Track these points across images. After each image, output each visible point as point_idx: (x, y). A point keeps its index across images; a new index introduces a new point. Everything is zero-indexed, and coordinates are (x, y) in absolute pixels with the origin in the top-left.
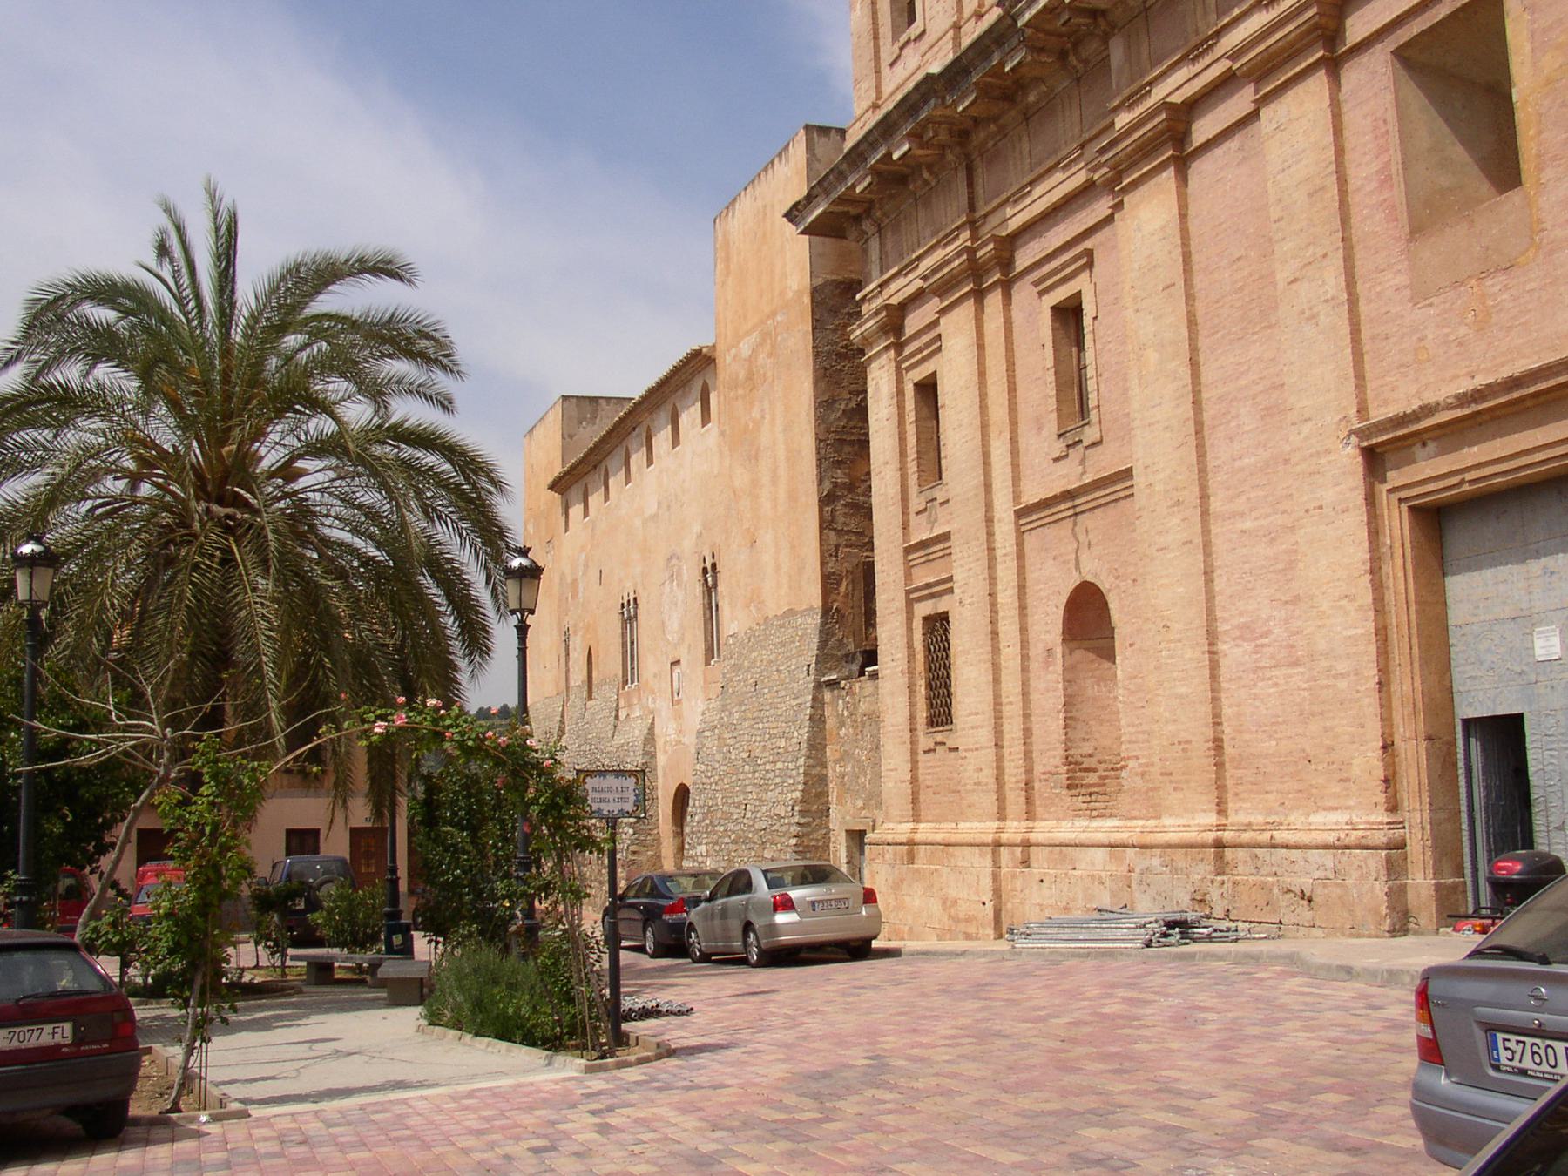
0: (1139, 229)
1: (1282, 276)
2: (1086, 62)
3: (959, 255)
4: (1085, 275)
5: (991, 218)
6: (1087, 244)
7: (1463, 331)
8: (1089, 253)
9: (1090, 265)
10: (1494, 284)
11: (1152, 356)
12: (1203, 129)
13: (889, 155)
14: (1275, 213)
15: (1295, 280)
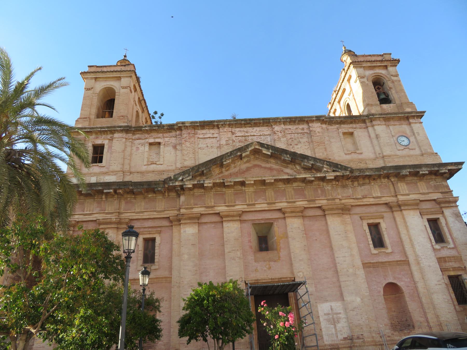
0: (185, 232)
1: (226, 251)
2: (169, 196)
3: (116, 218)
4: (157, 234)
5: (125, 214)
6: (159, 229)
7: (265, 269)
8: (161, 231)
9: (160, 233)
10: (272, 263)
11: (186, 256)
12: (204, 220)
13: (103, 190)
14: (225, 240)
15: (230, 252)
